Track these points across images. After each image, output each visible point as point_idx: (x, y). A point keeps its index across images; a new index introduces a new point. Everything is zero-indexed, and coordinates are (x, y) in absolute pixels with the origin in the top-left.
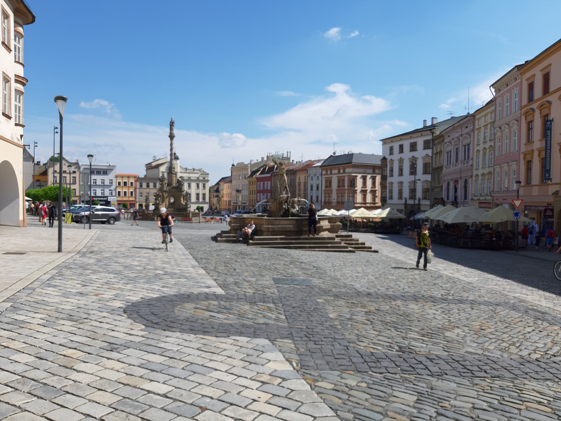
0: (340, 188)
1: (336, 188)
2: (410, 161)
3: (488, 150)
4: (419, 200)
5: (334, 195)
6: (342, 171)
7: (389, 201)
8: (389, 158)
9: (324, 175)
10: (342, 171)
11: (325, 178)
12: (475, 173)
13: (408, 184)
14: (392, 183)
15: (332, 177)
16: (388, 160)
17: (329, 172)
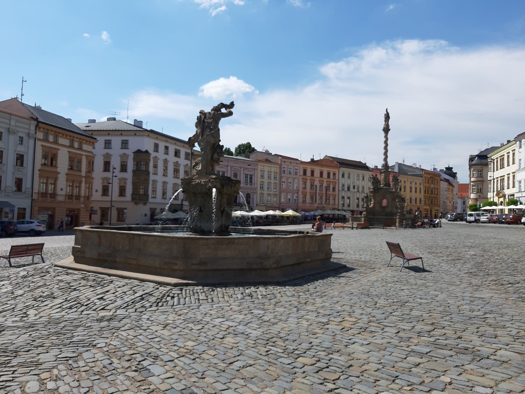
0: (72, 172)
1: (67, 172)
2: (175, 165)
3: (272, 184)
4: (182, 200)
5: (62, 183)
6: (76, 145)
7: (151, 200)
8: (153, 154)
9: (39, 140)
10: (76, 145)
11: (42, 146)
12: (259, 191)
13: (172, 186)
14: (155, 182)
15: (60, 149)
16: (152, 156)
17: (51, 138)
